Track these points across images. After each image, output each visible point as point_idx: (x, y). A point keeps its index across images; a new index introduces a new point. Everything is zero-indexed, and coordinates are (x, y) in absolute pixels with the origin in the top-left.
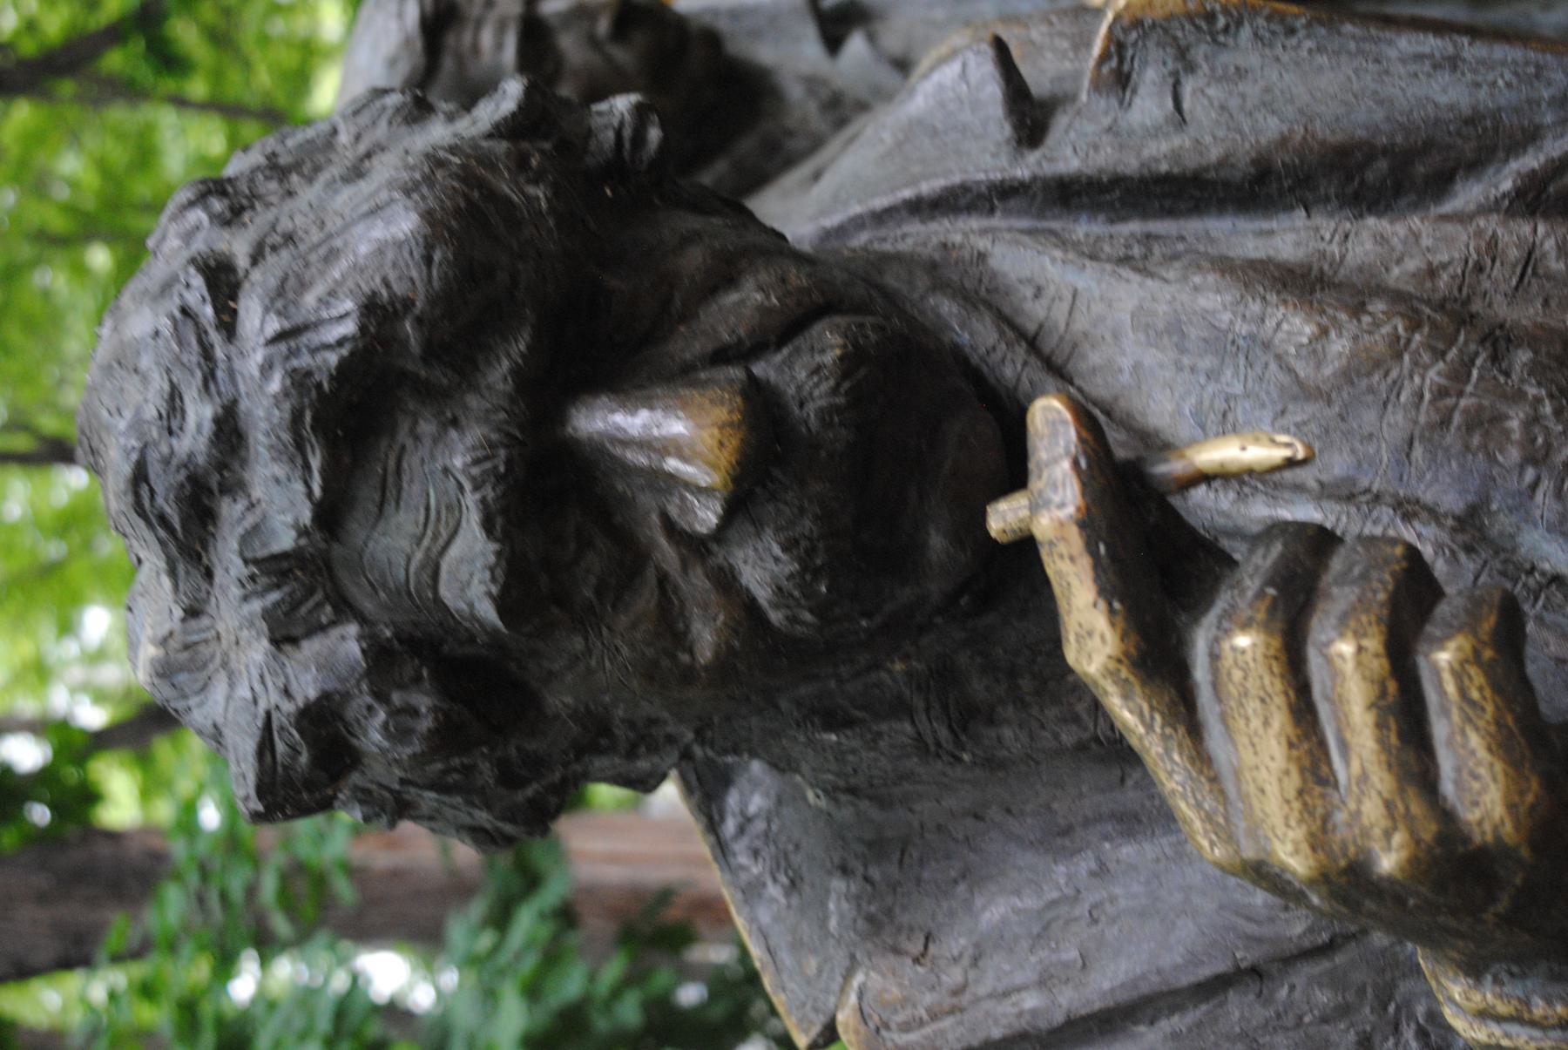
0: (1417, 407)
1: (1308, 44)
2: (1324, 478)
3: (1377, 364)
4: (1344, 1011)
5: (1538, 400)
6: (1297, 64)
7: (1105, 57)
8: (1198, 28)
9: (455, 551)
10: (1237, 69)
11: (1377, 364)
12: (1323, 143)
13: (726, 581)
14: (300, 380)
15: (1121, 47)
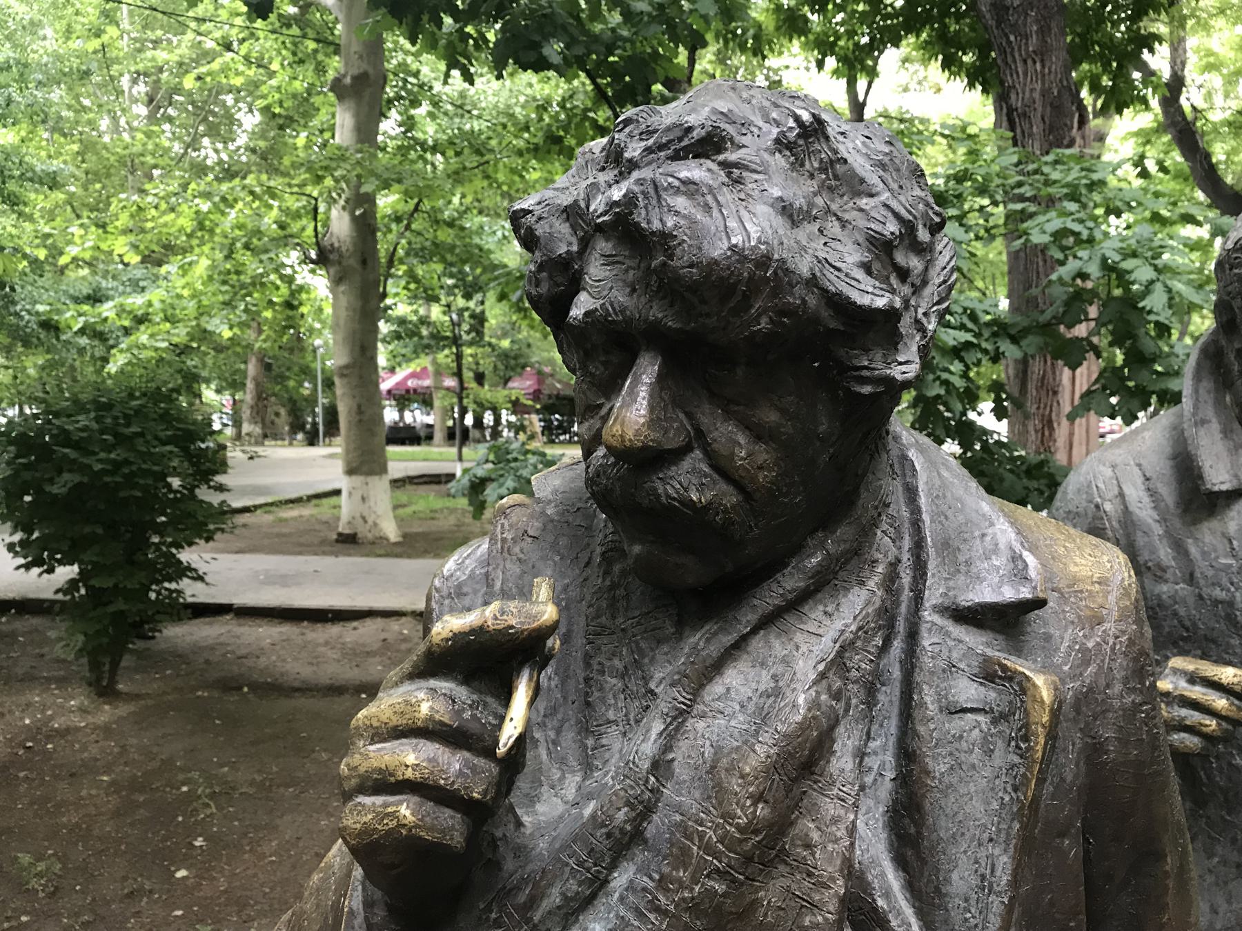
0: (696, 822)
1: (1007, 798)
2: (676, 763)
3: (720, 804)
5: (692, 890)
6: (993, 789)
7: (1004, 668)
8: (1020, 730)
10: (992, 751)
11: (720, 804)
12: (924, 796)
15: (1010, 679)
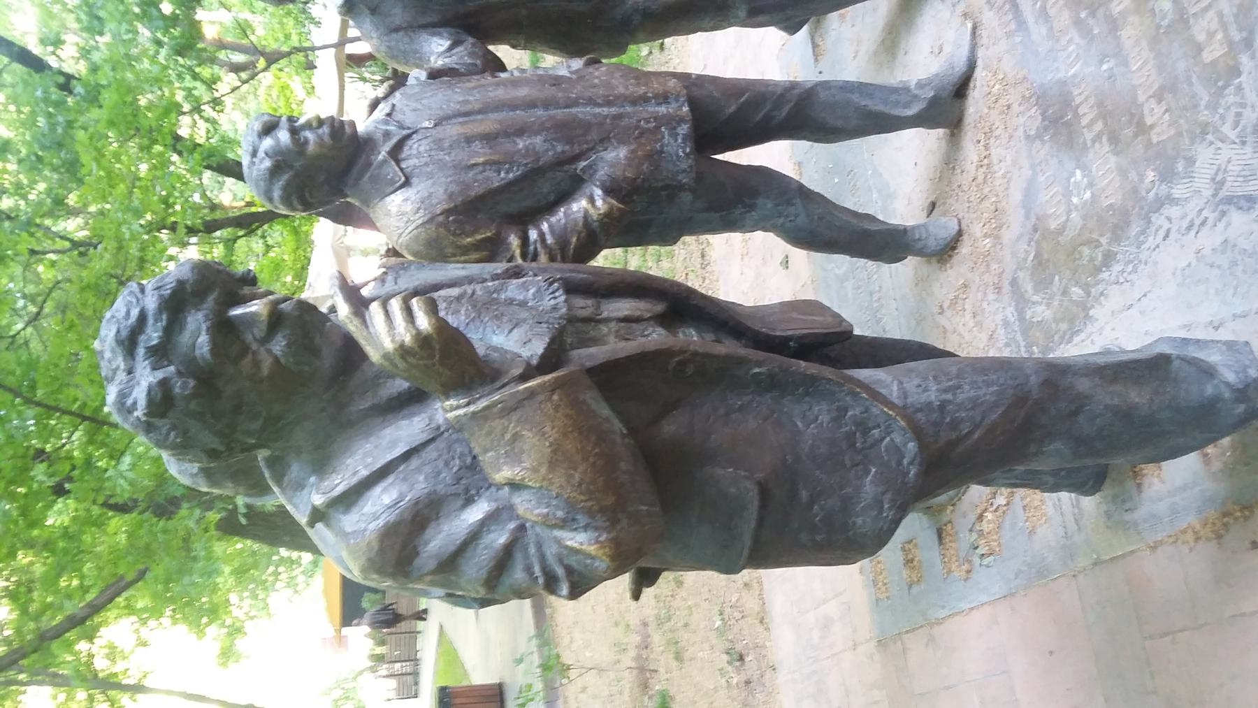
4: (440, 456)
9: (200, 340)
13: (269, 351)
14: (161, 296)
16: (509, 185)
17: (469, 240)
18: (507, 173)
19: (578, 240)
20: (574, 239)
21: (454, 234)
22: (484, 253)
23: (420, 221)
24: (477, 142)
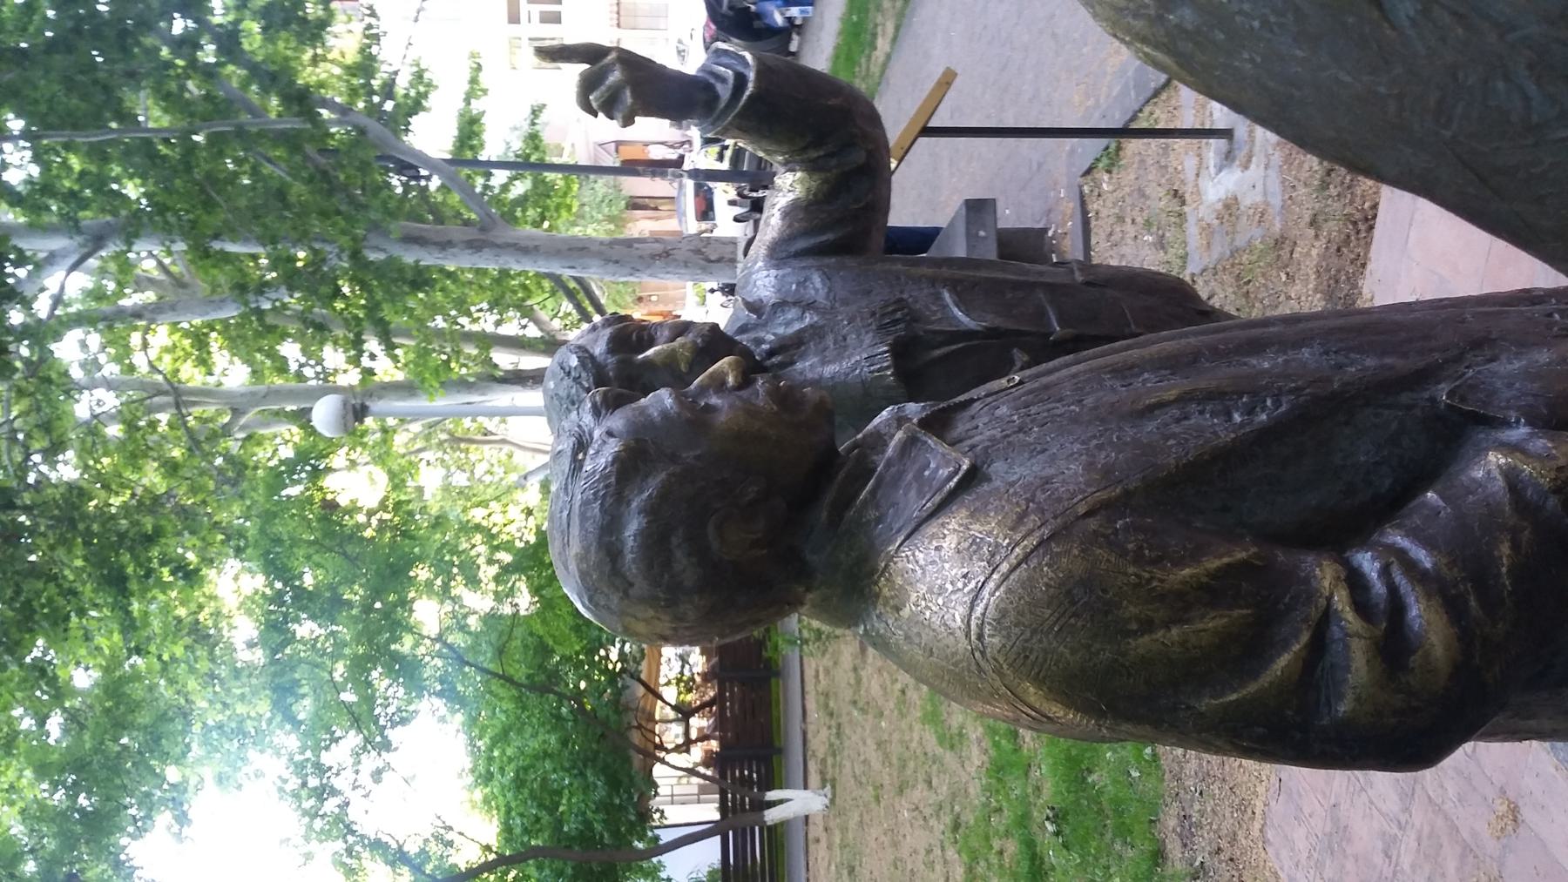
16: (1266, 436)
17: (1187, 571)
18: (1250, 411)
19: (1515, 546)
20: (1505, 549)
21: (1138, 559)
22: (1237, 613)
23: (1033, 541)
24: (1146, 375)
